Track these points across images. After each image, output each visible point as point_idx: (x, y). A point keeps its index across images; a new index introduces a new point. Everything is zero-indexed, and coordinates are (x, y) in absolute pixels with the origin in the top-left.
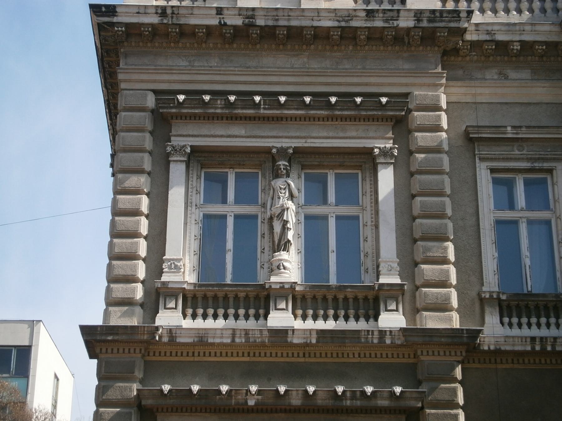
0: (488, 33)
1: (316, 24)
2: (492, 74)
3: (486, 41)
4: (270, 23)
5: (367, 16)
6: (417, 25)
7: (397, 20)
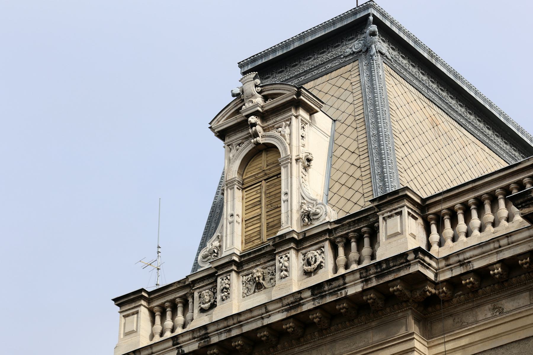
0: (462, 263)
1: (266, 322)
2: (485, 313)
3: (461, 275)
4: (223, 337)
5: (313, 295)
6: (365, 287)
7: (345, 288)
